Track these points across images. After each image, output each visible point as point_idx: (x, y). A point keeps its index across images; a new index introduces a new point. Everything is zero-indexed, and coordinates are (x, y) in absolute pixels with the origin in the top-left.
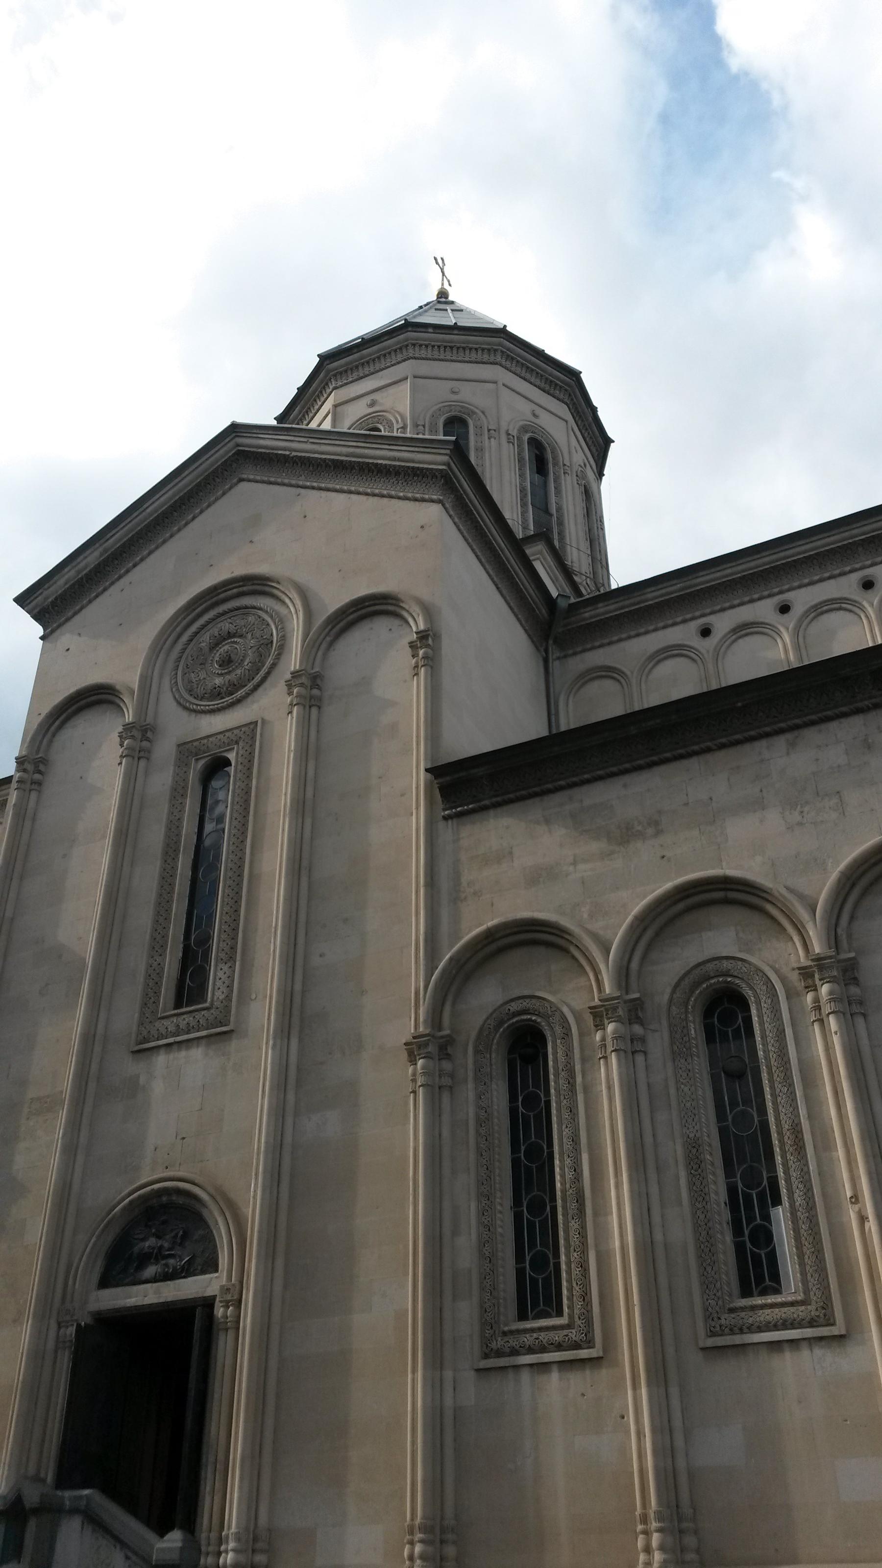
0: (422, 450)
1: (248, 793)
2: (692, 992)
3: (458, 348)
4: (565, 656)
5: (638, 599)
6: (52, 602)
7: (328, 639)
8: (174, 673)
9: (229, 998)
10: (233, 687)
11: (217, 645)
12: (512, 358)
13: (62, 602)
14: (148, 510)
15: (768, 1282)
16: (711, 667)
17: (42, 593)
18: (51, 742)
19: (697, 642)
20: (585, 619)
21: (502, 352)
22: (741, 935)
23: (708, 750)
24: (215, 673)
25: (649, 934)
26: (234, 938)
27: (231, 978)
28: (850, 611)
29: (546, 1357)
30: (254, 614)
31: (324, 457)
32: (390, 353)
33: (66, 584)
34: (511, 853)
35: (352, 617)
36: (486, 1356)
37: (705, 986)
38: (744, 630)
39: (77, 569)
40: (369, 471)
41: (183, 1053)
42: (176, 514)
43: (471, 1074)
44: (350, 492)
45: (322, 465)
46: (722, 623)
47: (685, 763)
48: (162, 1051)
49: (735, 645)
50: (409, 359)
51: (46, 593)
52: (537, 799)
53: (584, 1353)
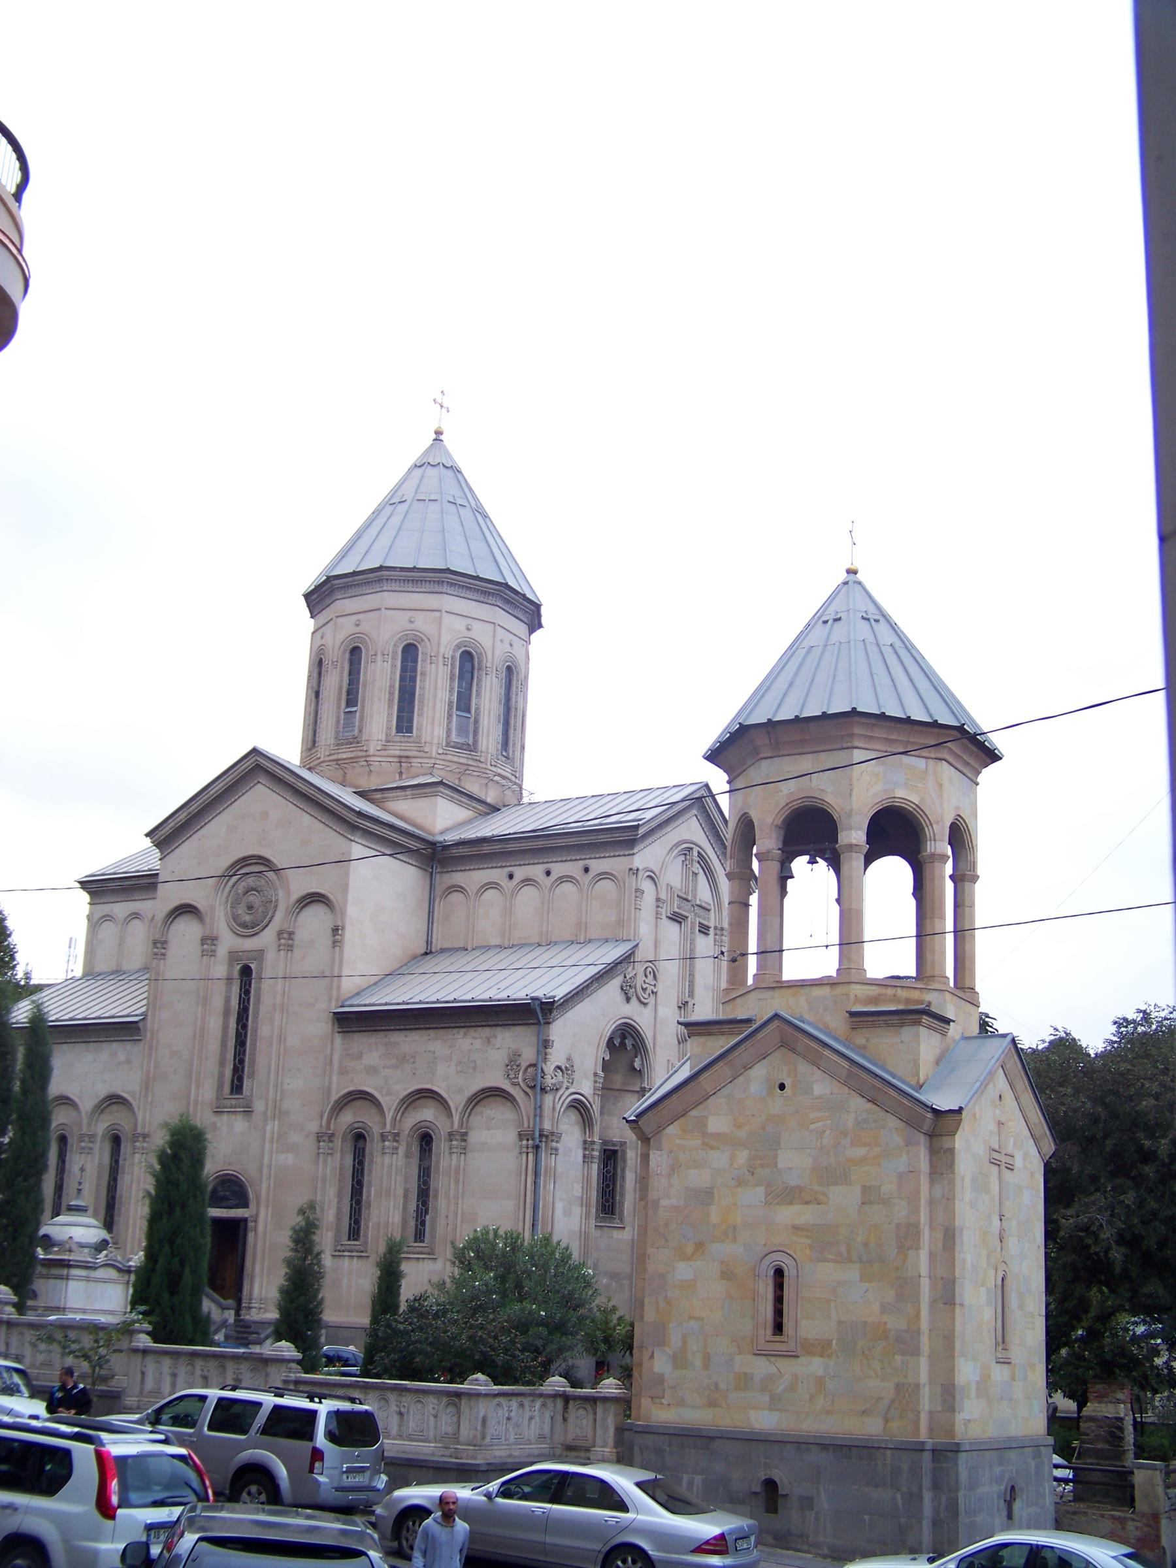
4: (442, 872)
5: (479, 849)
9: (251, 1095)
11: (247, 893)
12: (455, 584)
14: (211, 792)
23: (437, 1028)
25: (404, 1106)
27: (252, 1086)
29: (353, 1254)
36: (335, 1251)
38: (528, 881)
43: (339, 1150)
46: (520, 873)
49: (522, 889)
51: (160, 833)
53: (364, 1254)
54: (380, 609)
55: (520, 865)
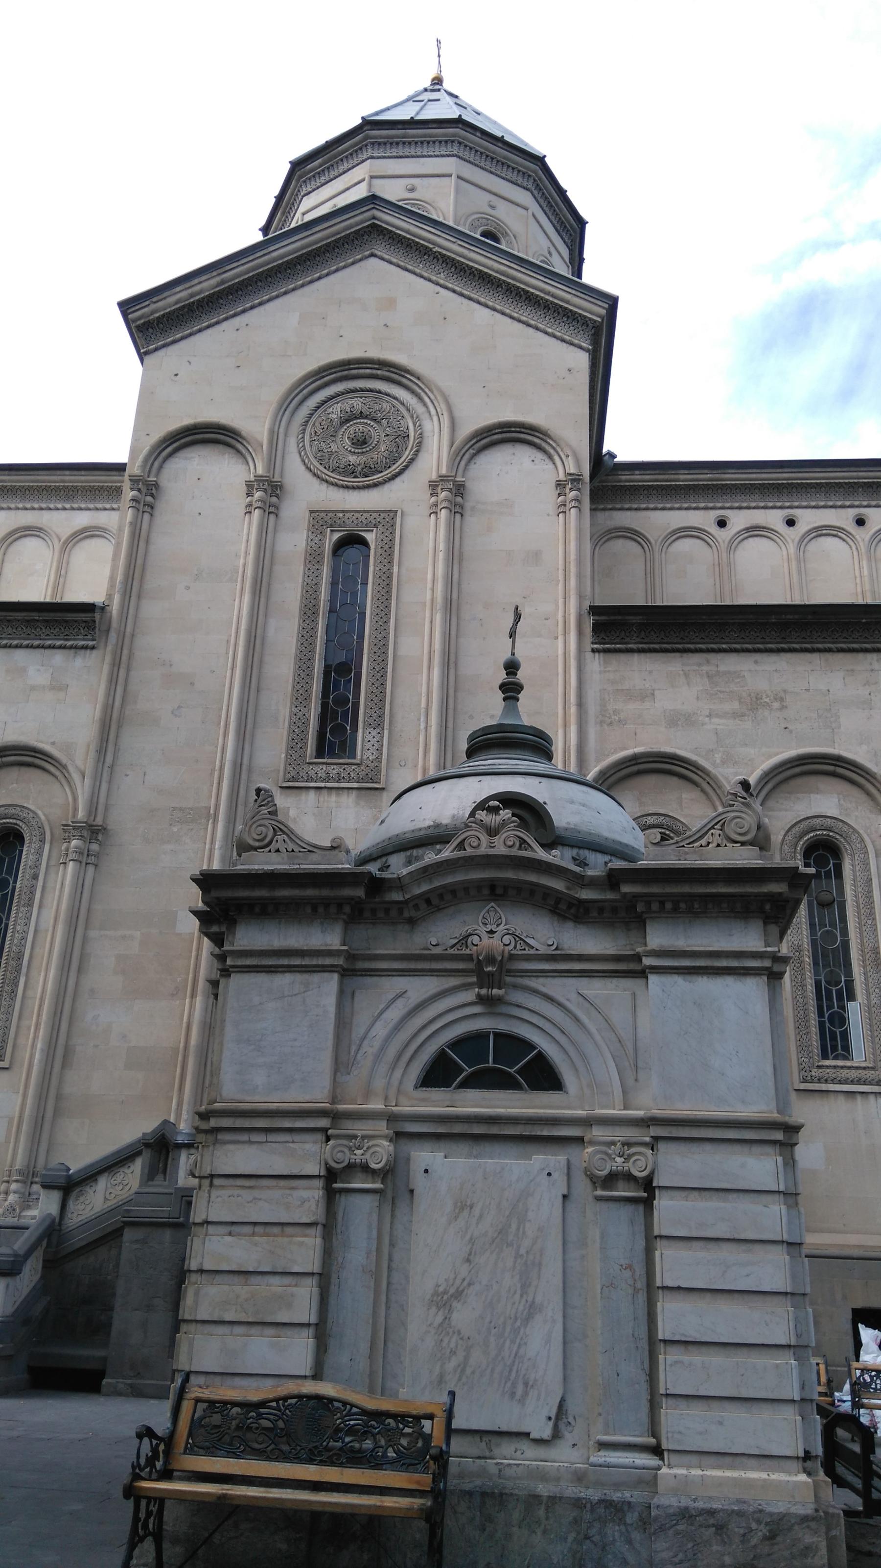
0: (579, 294)
1: (390, 577)
2: (801, 838)
3: (498, 161)
5: (672, 477)
6: (158, 318)
7: (471, 451)
8: (300, 436)
9: (379, 759)
10: (369, 470)
11: (348, 421)
13: (168, 320)
15: (840, 1051)
16: (724, 555)
17: (149, 305)
18: (161, 467)
19: (714, 529)
20: (620, 481)
21: (534, 180)
22: (842, 802)
23: (830, 650)
24: (347, 449)
25: (769, 786)
26: (382, 708)
27: (380, 742)
28: (844, 540)
30: (387, 402)
31: (471, 264)
32: (434, 142)
33: (176, 303)
34: (653, 694)
35: (496, 437)
37: (812, 835)
38: (755, 531)
39: (190, 291)
40: (517, 294)
41: (334, 797)
42: (299, 267)
44: (495, 310)
45: (465, 271)
46: (739, 520)
47: (808, 656)
48: (312, 794)
49: (745, 542)
50: (453, 156)
51: (153, 307)
52: (678, 655)
54: (450, 176)
55: (740, 508)
